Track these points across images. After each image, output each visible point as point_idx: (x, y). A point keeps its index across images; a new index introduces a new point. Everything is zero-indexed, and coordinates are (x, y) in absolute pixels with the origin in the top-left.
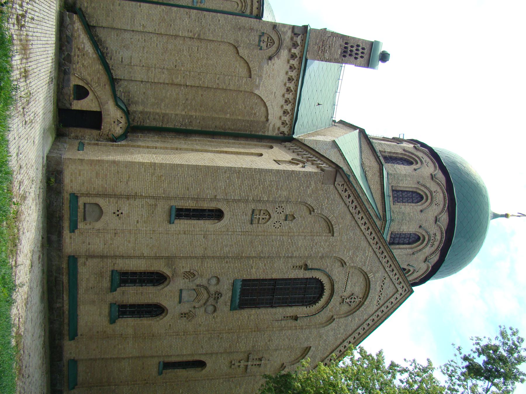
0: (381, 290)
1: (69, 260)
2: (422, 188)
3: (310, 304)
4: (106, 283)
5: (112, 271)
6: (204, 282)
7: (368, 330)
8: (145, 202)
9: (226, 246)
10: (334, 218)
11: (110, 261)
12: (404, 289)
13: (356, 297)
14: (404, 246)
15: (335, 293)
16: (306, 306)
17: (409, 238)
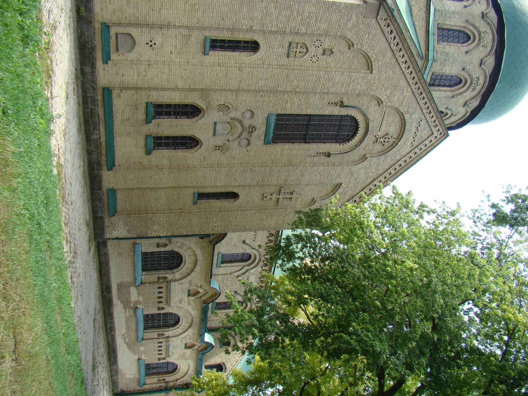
0: (416, 132)
1: (103, 92)
2: (471, 28)
3: (344, 142)
4: (141, 115)
5: (147, 103)
6: (238, 115)
7: (399, 171)
8: (178, 32)
9: (262, 80)
10: (374, 55)
11: (144, 93)
12: (439, 132)
13: (390, 138)
14: (445, 88)
16: (340, 143)
17: (451, 80)
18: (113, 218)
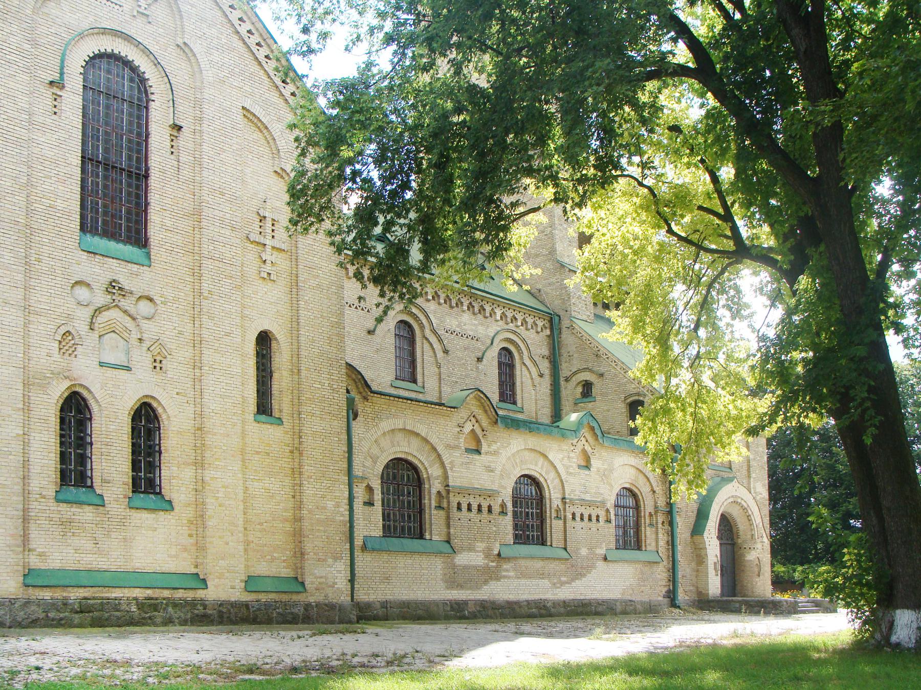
4: (87, 514)
5: (58, 501)
6: (86, 314)
11: (34, 505)
15: (123, 31)
18: (308, 586)
